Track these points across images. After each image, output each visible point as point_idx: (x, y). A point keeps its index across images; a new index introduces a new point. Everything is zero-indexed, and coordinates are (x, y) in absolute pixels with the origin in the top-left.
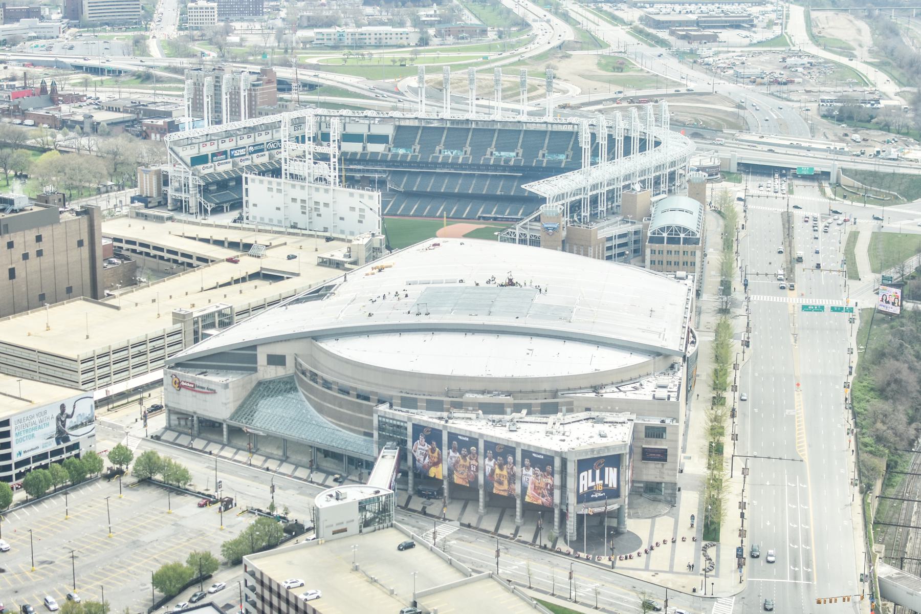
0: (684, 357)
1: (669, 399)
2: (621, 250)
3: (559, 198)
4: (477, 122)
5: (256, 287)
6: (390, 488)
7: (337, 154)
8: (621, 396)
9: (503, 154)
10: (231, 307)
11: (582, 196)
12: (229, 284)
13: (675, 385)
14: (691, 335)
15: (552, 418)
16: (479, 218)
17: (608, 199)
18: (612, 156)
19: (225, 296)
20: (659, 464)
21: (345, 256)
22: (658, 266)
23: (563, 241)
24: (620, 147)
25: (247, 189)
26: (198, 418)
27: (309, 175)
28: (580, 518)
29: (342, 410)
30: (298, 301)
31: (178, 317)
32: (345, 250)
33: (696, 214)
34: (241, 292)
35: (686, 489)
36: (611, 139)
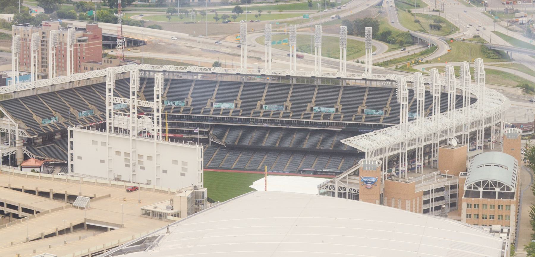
2: (438, 204)
3: (376, 153)
4: (297, 78)
5: (80, 238)
7: (160, 108)
9: (322, 109)
11: (400, 151)
12: (53, 235)
16: (300, 171)
17: (425, 154)
18: (429, 113)
19: (50, 247)
21: (168, 208)
22: (475, 219)
23: (381, 195)
24: (437, 103)
25: (72, 142)
27: (133, 127)
32: (168, 203)
33: (511, 169)
34: (65, 242)
36: (428, 96)
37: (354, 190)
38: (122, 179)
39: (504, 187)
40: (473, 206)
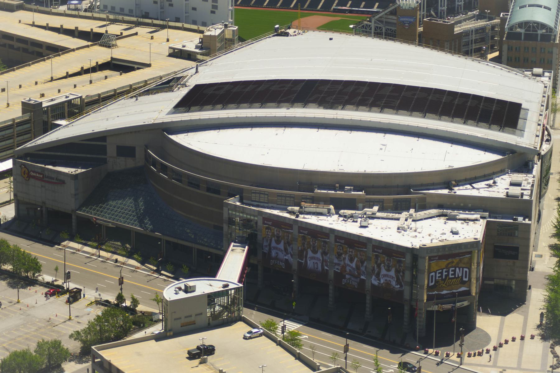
0: (539, 154)
1: (522, 195)
6: (240, 281)
8: (474, 193)
10: (81, 97)
13: (528, 183)
14: (546, 133)
15: (404, 214)
16: (335, 11)
19: (75, 86)
20: (510, 262)
21: (197, 47)
26: (47, 208)
28: (430, 314)
29: (191, 202)
30: (148, 92)
31: (26, 107)
32: (197, 41)
33: (554, 11)
35: (537, 287)
37: (391, 29)
38: (150, 16)
39: (547, 29)
40: (514, 49)
